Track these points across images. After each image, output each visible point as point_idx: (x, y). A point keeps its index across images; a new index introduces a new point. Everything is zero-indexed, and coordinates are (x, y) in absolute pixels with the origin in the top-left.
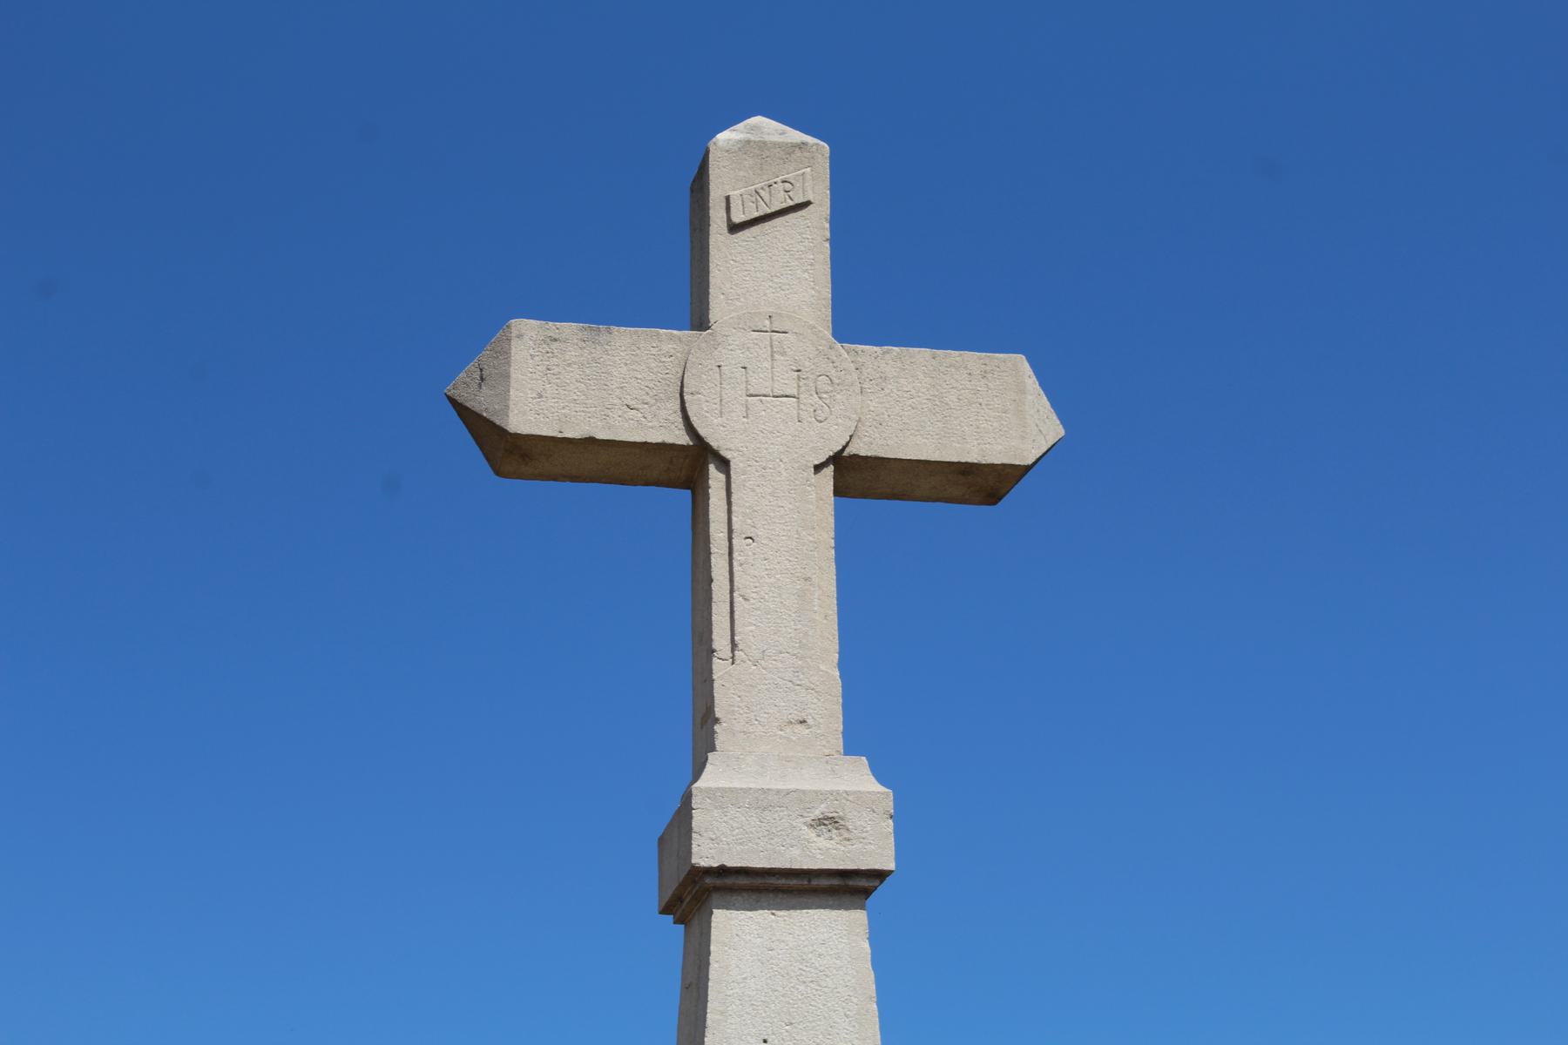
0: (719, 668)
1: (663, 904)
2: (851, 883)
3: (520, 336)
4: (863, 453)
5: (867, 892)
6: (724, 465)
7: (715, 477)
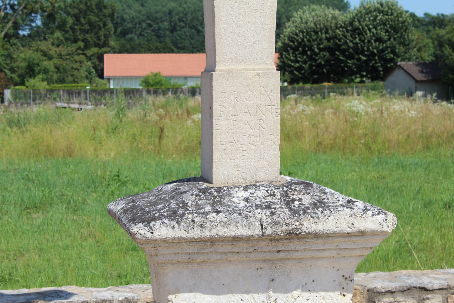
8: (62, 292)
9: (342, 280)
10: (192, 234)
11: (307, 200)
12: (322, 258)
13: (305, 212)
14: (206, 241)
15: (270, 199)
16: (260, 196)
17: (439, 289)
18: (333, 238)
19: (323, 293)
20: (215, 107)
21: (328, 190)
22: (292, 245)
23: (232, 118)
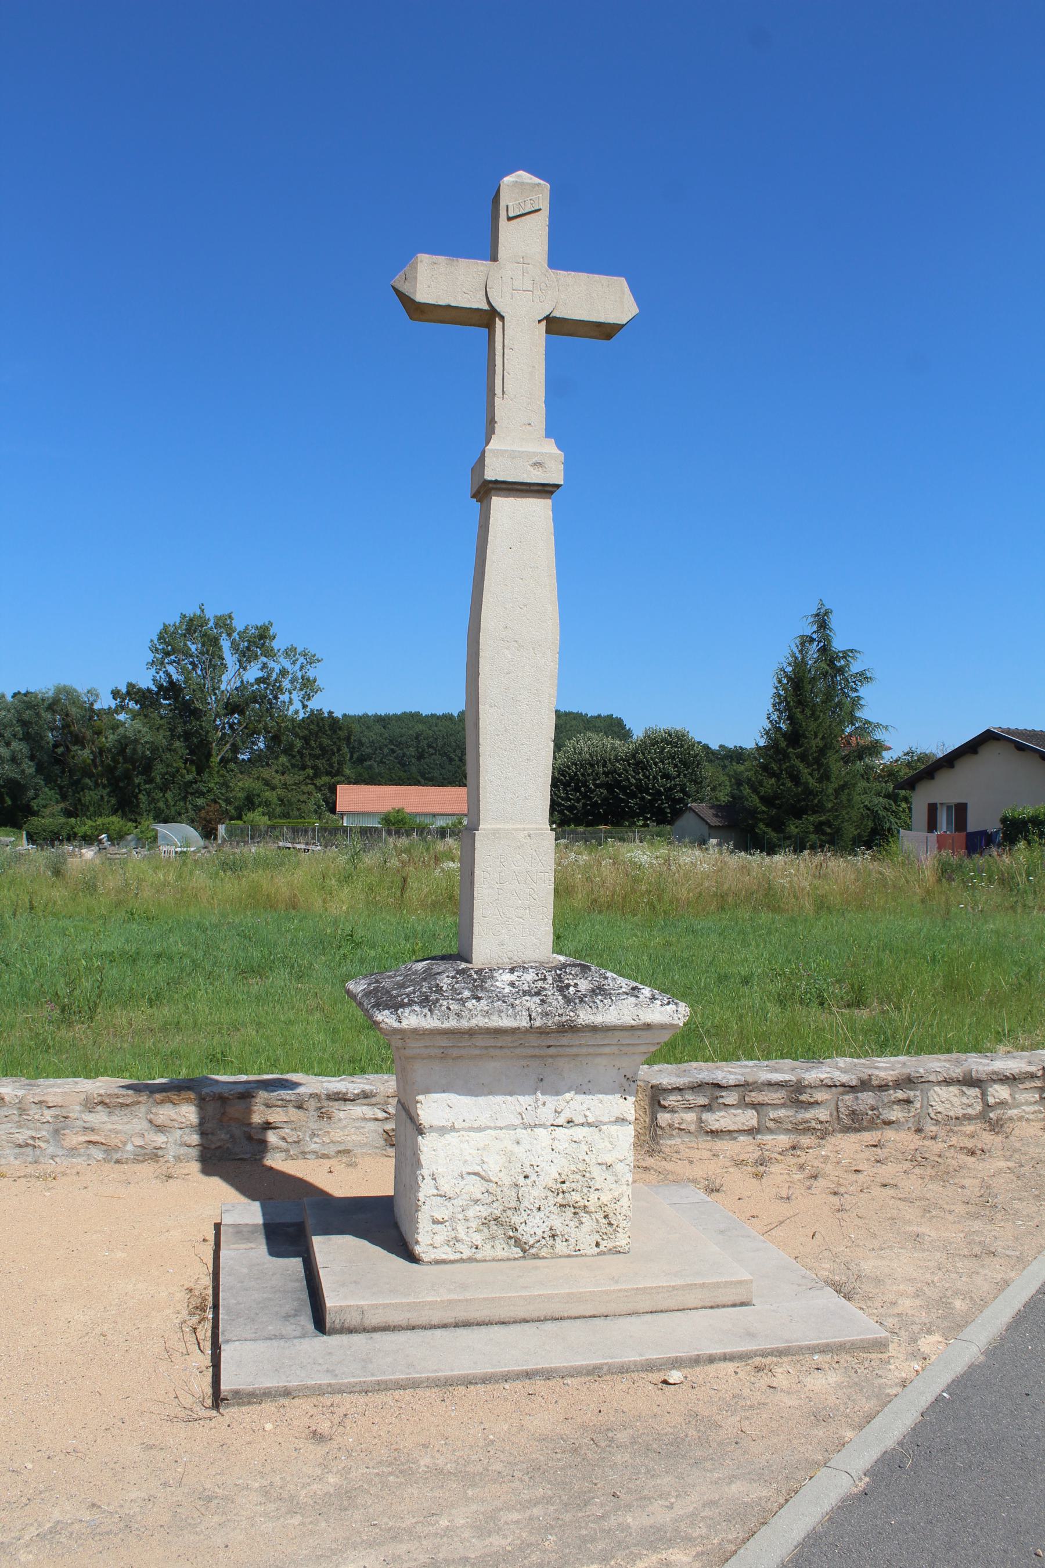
0: (498, 401)
2: (546, 489)
3: (421, 261)
5: (552, 493)
6: (502, 318)
7: (498, 323)
8: (287, 1080)
9: (624, 1081)
10: (447, 1025)
11: (584, 985)
12: (601, 1054)
14: (463, 1033)
15: (540, 984)
16: (528, 980)
17: (735, 1086)
18: (614, 1032)
19: (600, 1096)
20: (477, 872)
21: (609, 974)
22: (565, 1040)
23: (497, 886)
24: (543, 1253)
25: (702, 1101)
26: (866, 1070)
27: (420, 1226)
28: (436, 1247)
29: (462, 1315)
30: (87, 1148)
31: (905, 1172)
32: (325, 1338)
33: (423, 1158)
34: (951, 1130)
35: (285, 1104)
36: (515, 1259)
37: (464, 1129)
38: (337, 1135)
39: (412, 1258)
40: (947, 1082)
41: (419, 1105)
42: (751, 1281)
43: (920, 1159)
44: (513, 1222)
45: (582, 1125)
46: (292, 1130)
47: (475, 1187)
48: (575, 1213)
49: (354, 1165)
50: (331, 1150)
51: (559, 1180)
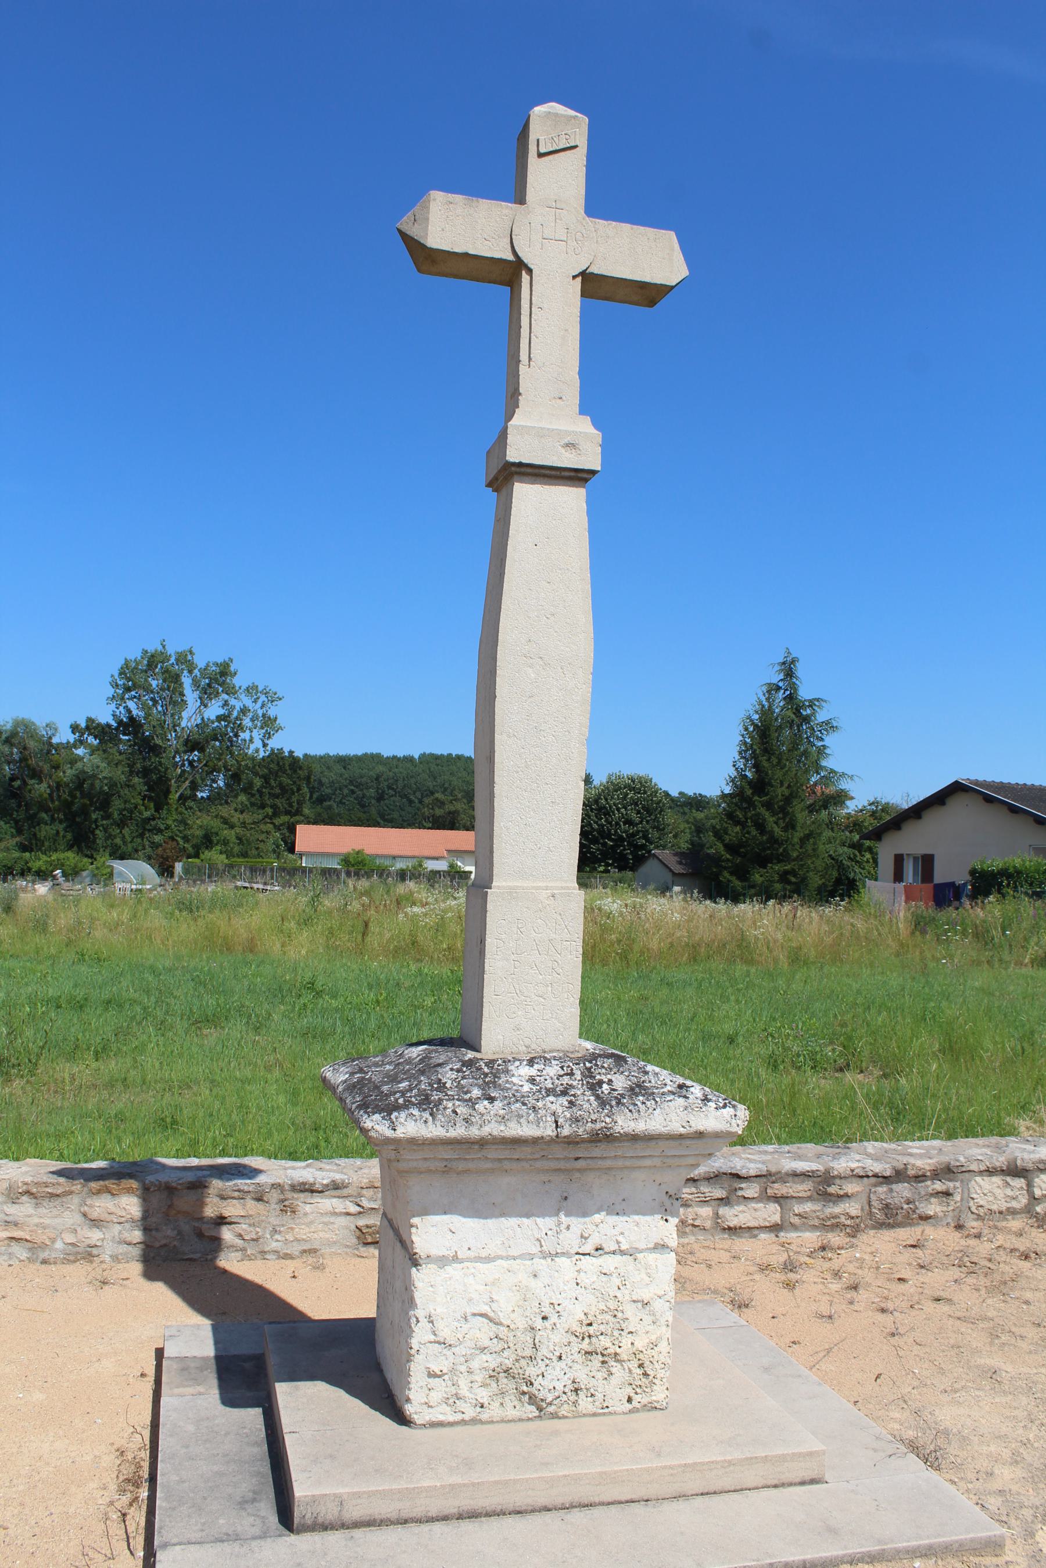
0: (523, 369)
1: (490, 479)
2: (579, 475)
3: (434, 200)
4: (595, 272)
5: (586, 480)
6: (530, 271)
7: (525, 277)
8: (245, 1166)
9: (665, 1198)
10: (453, 1133)
11: (620, 1082)
12: (640, 1167)
13: (619, 1103)
14: (473, 1143)
15: (566, 1080)
16: (551, 1074)
17: (756, 1176)
18: (658, 1141)
19: (636, 1217)
20: (489, 940)
21: (649, 1068)
22: (597, 1151)
23: (513, 957)
24: (563, 1412)
25: (719, 1193)
26: (899, 1158)
27: (412, 1380)
28: (431, 1407)
29: (466, 1502)
30: (9, 1245)
31: (956, 1281)
32: (293, 1538)
33: (418, 1296)
34: (996, 1227)
35: (242, 1195)
36: (529, 1419)
37: (469, 1260)
38: (302, 1231)
39: (401, 1418)
40: (990, 1172)
41: (413, 1230)
42: (824, 1452)
43: (968, 1264)
44: (527, 1374)
45: (614, 1252)
46: (250, 1225)
47: (481, 1332)
48: (603, 1362)
49: (319, 1268)
50: (295, 1249)
51: (585, 1322)
